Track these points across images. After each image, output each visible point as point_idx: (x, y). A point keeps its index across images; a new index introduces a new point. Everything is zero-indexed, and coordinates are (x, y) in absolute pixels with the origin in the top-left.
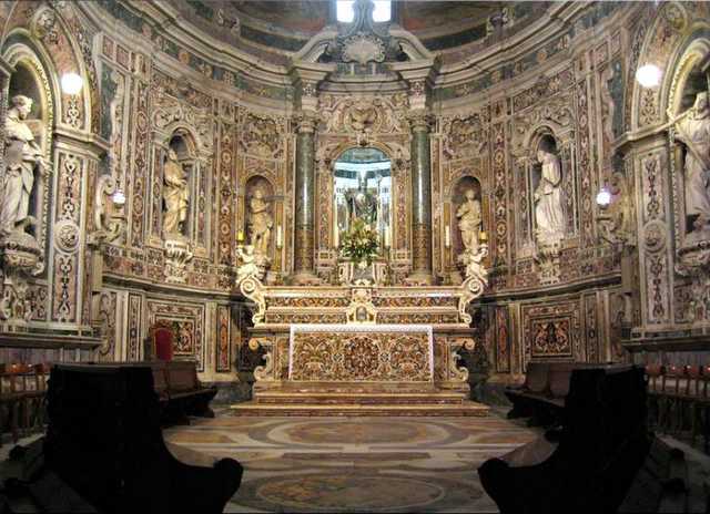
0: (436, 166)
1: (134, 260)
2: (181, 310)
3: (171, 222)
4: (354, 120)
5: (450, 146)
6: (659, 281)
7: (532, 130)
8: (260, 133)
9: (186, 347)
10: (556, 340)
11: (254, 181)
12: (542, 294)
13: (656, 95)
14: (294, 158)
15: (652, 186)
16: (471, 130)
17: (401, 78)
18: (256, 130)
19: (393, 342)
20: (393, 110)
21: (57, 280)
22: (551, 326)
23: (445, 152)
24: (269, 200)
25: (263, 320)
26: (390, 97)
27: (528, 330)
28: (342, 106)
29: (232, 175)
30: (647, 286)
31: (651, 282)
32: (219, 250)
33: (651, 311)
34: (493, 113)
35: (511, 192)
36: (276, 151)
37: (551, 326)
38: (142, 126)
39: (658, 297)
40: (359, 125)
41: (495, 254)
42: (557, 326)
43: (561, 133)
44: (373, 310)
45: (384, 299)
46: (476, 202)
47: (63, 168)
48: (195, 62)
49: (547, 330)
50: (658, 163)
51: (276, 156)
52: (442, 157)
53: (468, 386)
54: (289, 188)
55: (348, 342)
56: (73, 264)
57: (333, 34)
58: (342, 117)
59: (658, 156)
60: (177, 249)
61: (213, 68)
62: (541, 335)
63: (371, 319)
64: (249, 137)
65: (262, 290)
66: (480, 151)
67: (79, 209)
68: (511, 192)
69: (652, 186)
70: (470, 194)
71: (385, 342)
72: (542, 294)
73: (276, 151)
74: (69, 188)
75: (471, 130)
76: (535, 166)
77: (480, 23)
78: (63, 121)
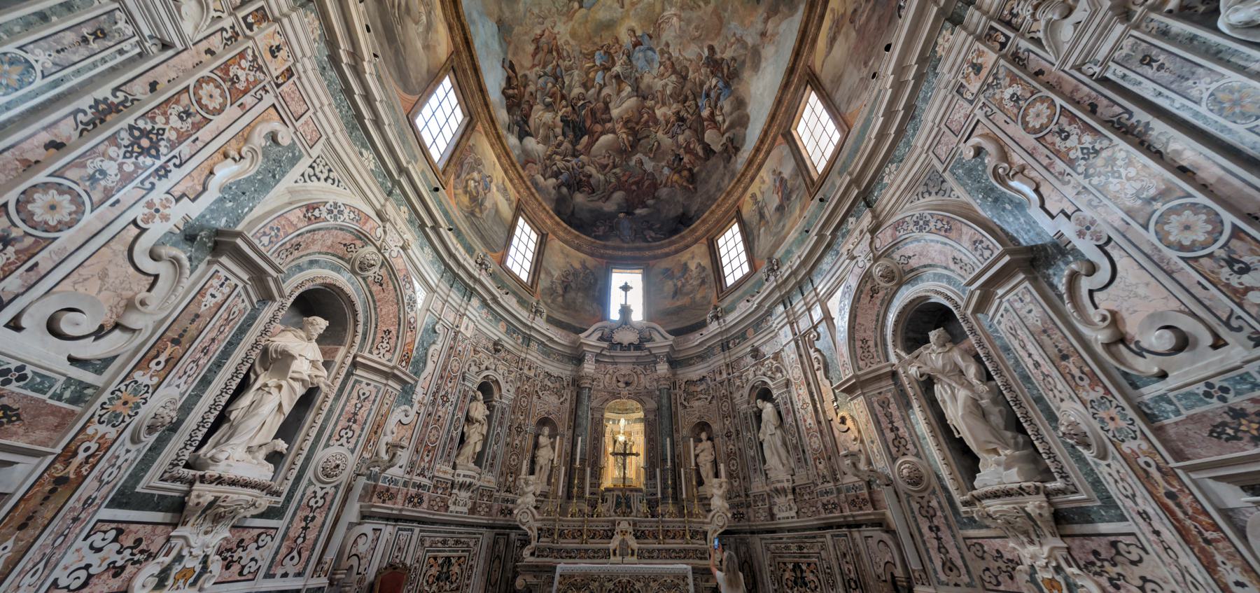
0: (676, 413)
1: (413, 491)
2: (457, 542)
3: (468, 450)
6: (938, 529)
8: (551, 386)
9: (454, 586)
11: (543, 422)
12: (781, 530)
13: (871, 343)
14: (574, 406)
16: (701, 387)
17: (651, 354)
18: (549, 384)
21: (297, 518)
22: (797, 566)
24: (552, 436)
25: (532, 554)
27: (772, 568)
28: (611, 372)
29: (527, 416)
30: (922, 535)
31: (925, 530)
32: (506, 480)
35: (738, 434)
38: (455, 369)
39: (941, 548)
40: (622, 385)
44: (633, 543)
45: (643, 532)
46: (709, 442)
47: (355, 394)
48: (511, 330)
49: (794, 570)
50: (892, 400)
52: (680, 408)
54: (569, 428)
56: (329, 498)
59: (889, 395)
60: (465, 479)
61: (524, 338)
62: (787, 575)
63: (633, 554)
64: (544, 388)
65: (536, 520)
66: (710, 403)
67: (360, 436)
68: (738, 434)
69: (892, 422)
70: (704, 436)
73: (562, 400)
74: (355, 414)
75: (701, 387)
76: (755, 413)
78: (371, 352)
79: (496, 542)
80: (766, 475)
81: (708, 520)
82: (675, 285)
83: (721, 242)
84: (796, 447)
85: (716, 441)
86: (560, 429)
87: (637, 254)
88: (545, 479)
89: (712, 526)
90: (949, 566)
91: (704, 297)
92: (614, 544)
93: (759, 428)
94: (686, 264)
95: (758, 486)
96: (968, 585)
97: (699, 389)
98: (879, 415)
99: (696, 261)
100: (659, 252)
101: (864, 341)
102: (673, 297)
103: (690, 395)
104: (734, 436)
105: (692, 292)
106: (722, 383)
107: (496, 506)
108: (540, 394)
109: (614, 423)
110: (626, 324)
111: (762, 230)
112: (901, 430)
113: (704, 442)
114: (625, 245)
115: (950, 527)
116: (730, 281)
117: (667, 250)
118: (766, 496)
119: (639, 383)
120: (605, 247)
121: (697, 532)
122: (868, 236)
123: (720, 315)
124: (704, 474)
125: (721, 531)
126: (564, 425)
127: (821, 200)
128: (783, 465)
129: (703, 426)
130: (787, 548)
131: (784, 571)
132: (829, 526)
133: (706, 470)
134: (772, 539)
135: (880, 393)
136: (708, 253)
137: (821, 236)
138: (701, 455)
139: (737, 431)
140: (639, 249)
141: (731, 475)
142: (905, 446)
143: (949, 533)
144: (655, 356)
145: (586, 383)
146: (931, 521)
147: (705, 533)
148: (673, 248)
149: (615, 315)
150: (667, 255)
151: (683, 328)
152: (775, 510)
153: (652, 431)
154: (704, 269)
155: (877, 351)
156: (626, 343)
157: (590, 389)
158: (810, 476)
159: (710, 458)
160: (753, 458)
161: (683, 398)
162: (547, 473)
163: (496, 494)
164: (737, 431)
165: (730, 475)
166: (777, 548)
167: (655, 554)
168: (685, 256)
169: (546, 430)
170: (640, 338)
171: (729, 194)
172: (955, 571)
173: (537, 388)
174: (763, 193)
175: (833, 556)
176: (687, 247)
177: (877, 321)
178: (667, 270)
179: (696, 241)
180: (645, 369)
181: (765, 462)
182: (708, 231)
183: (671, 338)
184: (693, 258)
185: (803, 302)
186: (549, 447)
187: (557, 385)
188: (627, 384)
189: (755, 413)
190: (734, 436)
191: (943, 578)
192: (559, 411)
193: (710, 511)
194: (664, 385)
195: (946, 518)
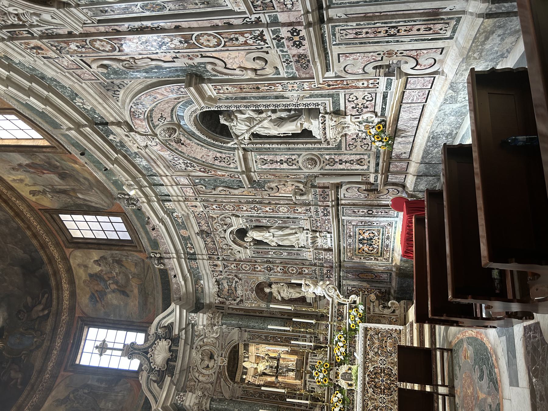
4: (208, 367)
5: (235, 300)
6: (340, 160)
7: (231, 243)
10: (371, 239)
12: (339, 246)
13: (218, 155)
15: (277, 162)
16: (225, 285)
23: (238, 304)
26: (196, 339)
28: (197, 375)
30: (343, 169)
31: (341, 167)
33: (361, 167)
34: (217, 269)
35: (270, 262)
37: (361, 241)
39: (351, 162)
41: (308, 276)
42: (361, 237)
43: (238, 224)
46: (273, 286)
49: (363, 244)
50: (262, 157)
53: (402, 302)
55: (371, 390)
57: (145, 374)
59: (258, 157)
62: (366, 249)
66: (240, 279)
68: (270, 262)
69: (277, 162)
72: (339, 246)
75: (225, 285)
76: (255, 244)
77: (158, 273)
80: (302, 247)
81: (330, 300)
82: (114, 291)
83: (76, 234)
84: (285, 222)
85: (272, 280)
87: (62, 330)
89: (335, 298)
90: (360, 162)
91: (136, 265)
93: (266, 244)
94: (91, 276)
95: (309, 255)
96: (369, 157)
97: (227, 287)
98: (271, 167)
99: (91, 263)
100: (66, 303)
101: (216, 158)
102: (128, 296)
103: (232, 293)
104: (271, 265)
105: (126, 276)
106: (225, 267)
109: (246, 374)
110: (147, 353)
111: (80, 196)
112: (282, 158)
113: (272, 290)
114: (46, 344)
115: (340, 154)
116: (126, 236)
117: (66, 294)
118: (316, 251)
120: (41, 371)
121: (338, 310)
122: (132, 133)
123: (158, 255)
124: (298, 296)
125: (338, 291)
127: (82, 154)
128: (296, 233)
129: (259, 289)
130: (350, 245)
131: (363, 250)
132: (338, 216)
133: (294, 294)
134: (344, 254)
135: (256, 162)
136: (86, 250)
137: (116, 161)
138: (282, 295)
139: (267, 261)
140: (55, 329)
141: (300, 273)
142: (293, 160)
143: (343, 156)
144: (187, 325)
146: (337, 162)
147: (339, 304)
148: (65, 286)
149: (134, 364)
150: (73, 294)
151: (163, 294)
152: (326, 247)
153: (259, 337)
154: (103, 258)
155: (225, 153)
156: (168, 355)
157: (213, 400)
158: (305, 218)
159: (285, 288)
160: (289, 253)
164: (266, 262)
165: (300, 274)
166: (350, 252)
167: (352, 350)
168: (81, 274)
171: (18, 214)
172: (362, 160)
174: (35, 184)
175: (354, 218)
176: (69, 270)
177: (202, 146)
178: (92, 297)
179: (66, 260)
181: (293, 246)
182: (57, 245)
183: (173, 305)
184: (86, 266)
185: (170, 188)
188: (211, 357)
189: (255, 244)
190: (271, 265)
191: (365, 167)
193: (324, 297)
195: (335, 154)
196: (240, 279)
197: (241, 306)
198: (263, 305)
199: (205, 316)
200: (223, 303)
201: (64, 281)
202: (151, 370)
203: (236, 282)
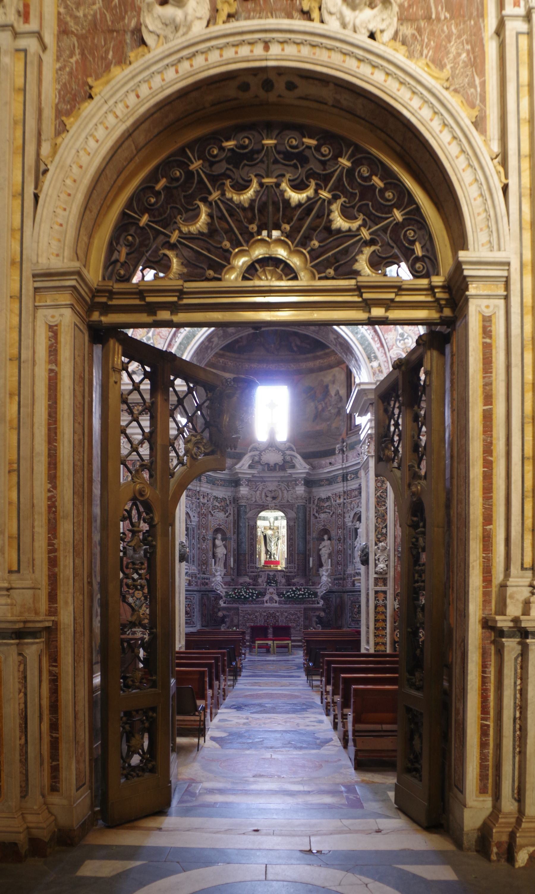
0: (309, 521)
5: (317, 512)
8: (219, 505)
11: (217, 531)
16: (327, 504)
18: (217, 504)
19: (286, 614)
20: (288, 491)
23: (314, 515)
36: (227, 514)
40: (269, 499)
44: (276, 598)
46: (329, 542)
51: (227, 517)
52: (312, 518)
55: (265, 614)
58: (261, 494)
63: (276, 602)
64: (214, 507)
66: (331, 516)
70: (326, 537)
71: (282, 614)
73: (227, 514)
75: (327, 504)
77: (332, 447)
79: (202, 598)
86: (228, 535)
88: (222, 565)
92: (266, 598)
94: (327, 386)
97: (325, 505)
102: (313, 421)
106: (339, 504)
107: (199, 582)
108: (212, 512)
119: (283, 498)
126: (230, 531)
145: (243, 502)
157: (245, 506)
159: (328, 551)
161: (315, 511)
162: (223, 562)
163: (198, 576)
169: (219, 536)
170: (284, 460)
173: (210, 509)
176: (330, 367)
180: (288, 486)
184: (334, 382)
186: (223, 547)
187: (223, 504)
192: (226, 523)
194: (301, 502)
196: (331, 516)
197: (312, 518)
198: (315, 535)
199: (302, 492)
200: (314, 503)
201: (321, 361)
202: (260, 455)
203: (329, 513)
